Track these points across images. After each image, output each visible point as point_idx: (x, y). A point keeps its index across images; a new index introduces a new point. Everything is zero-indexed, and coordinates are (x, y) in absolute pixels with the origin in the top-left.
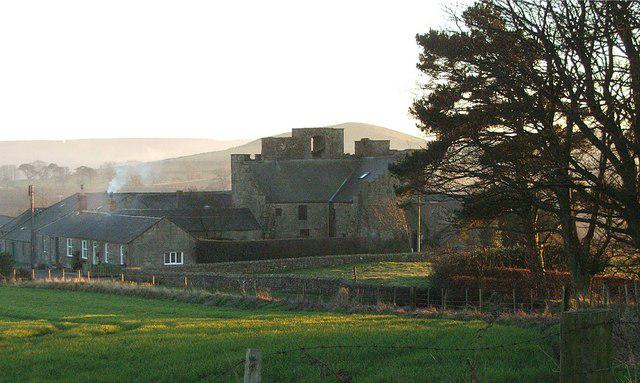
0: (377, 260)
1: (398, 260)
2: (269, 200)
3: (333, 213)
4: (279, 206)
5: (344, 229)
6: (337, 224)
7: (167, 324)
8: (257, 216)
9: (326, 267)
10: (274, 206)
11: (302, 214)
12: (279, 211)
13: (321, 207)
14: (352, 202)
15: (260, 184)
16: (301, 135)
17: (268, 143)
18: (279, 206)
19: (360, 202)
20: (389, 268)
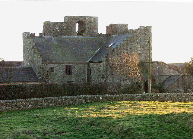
0: (114, 99)
1: (132, 99)
2: (44, 61)
3: (89, 71)
4: (52, 65)
5: (95, 79)
6: (92, 77)
7: (17, 130)
8: (36, 72)
9: (69, 106)
10: (48, 66)
11: (68, 71)
12: (52, 69)
13: (81, 66)
14: (101, 62)
15: (39, 50)
16: (70, 20)
17: (48, 26)
18: (52, 65)
19: (107, 60)
20: (125, 107)
